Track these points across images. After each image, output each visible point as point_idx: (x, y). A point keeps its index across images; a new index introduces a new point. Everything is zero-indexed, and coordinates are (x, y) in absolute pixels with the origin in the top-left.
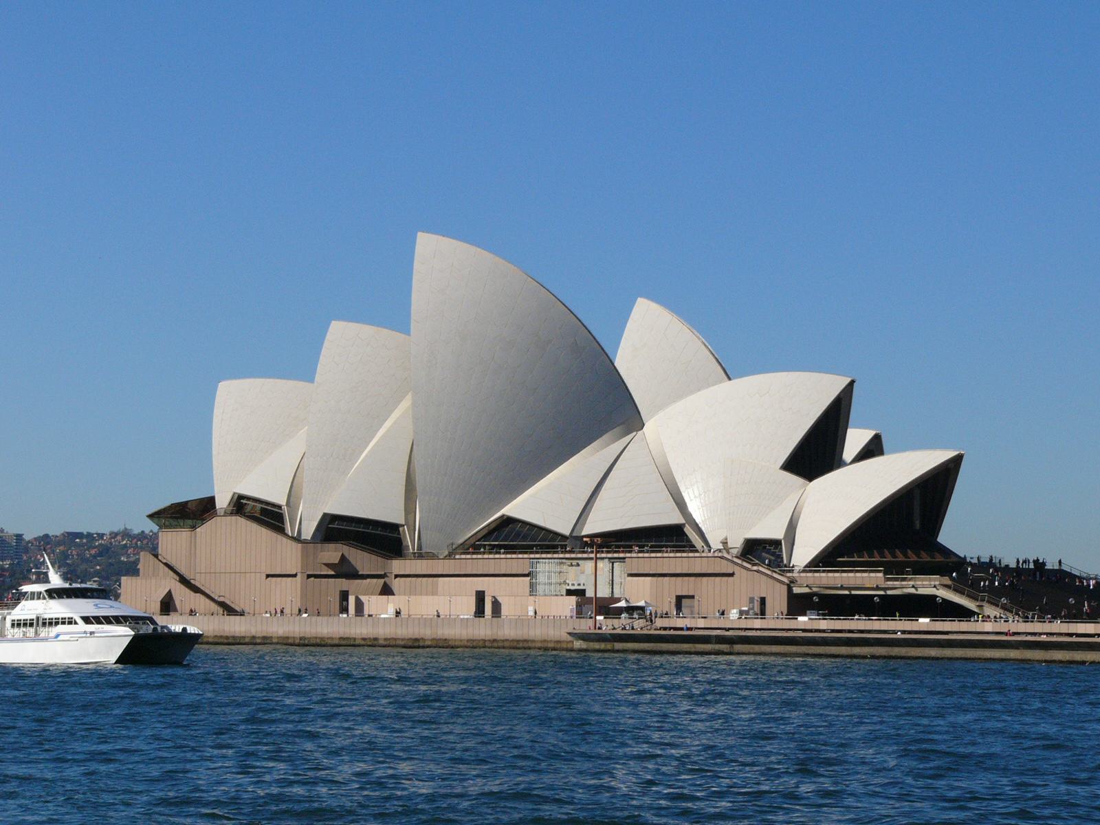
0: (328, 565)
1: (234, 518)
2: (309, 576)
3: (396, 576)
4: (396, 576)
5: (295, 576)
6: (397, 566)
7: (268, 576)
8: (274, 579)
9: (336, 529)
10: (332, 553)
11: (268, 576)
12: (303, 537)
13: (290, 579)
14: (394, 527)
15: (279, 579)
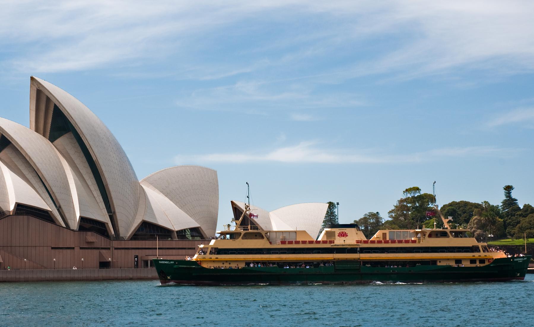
0: (88, 243)
1: (26, 217)
2: (81, 248)
3: (116, 249)
4: (116, 249)
5: (73, 248)
6: (115, 244)
7: (52, 248)
8: (57, 251)
9: (87, 224)
10: (92, 237)
11: (52, 248)
12: (72, 228)
13: (69, 251)
14: (102, 224)
15: (61, 250)
